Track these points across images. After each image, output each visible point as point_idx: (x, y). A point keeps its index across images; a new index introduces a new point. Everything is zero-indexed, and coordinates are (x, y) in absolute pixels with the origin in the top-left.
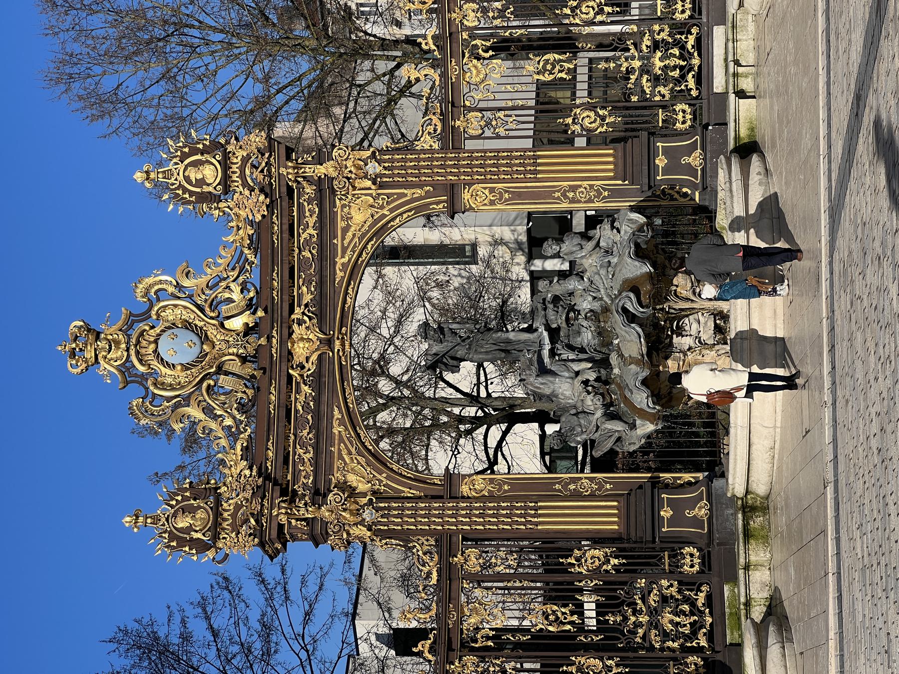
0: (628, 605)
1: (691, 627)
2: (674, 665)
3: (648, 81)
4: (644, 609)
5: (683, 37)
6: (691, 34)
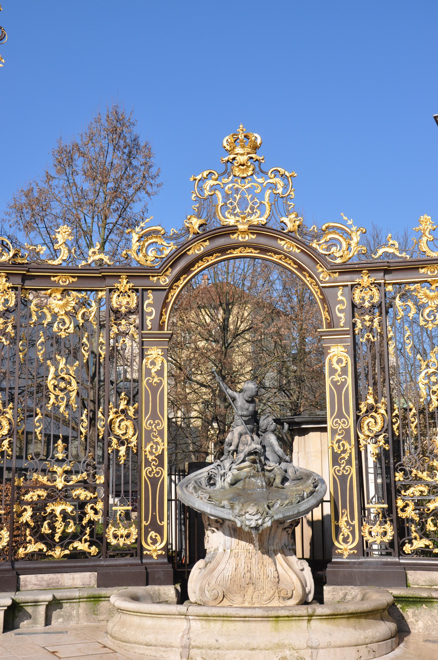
3: (39, 496)
5: (86, 537)
6: (90, 546)
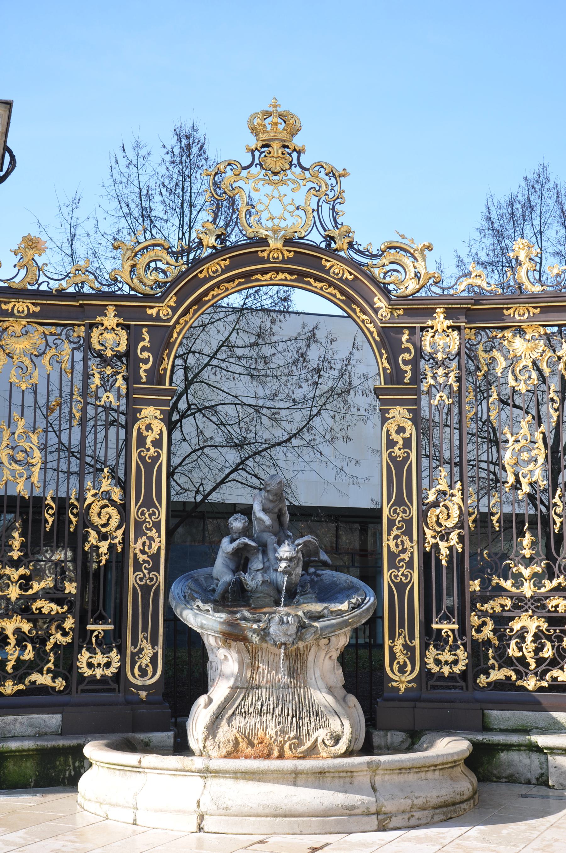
0: (548, 566)
1: (517, 659)
2: (453, 631)
4: (543, 590)
